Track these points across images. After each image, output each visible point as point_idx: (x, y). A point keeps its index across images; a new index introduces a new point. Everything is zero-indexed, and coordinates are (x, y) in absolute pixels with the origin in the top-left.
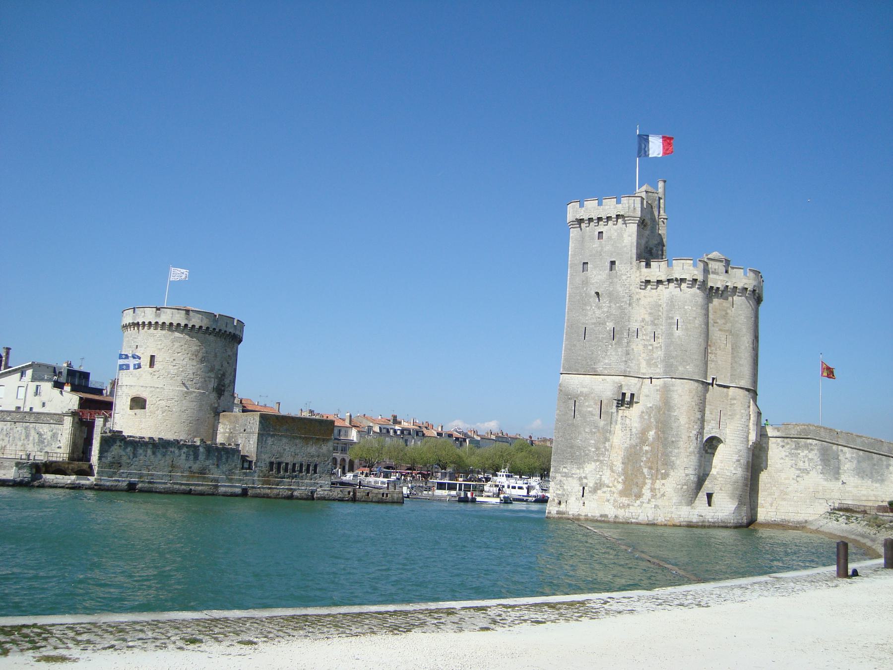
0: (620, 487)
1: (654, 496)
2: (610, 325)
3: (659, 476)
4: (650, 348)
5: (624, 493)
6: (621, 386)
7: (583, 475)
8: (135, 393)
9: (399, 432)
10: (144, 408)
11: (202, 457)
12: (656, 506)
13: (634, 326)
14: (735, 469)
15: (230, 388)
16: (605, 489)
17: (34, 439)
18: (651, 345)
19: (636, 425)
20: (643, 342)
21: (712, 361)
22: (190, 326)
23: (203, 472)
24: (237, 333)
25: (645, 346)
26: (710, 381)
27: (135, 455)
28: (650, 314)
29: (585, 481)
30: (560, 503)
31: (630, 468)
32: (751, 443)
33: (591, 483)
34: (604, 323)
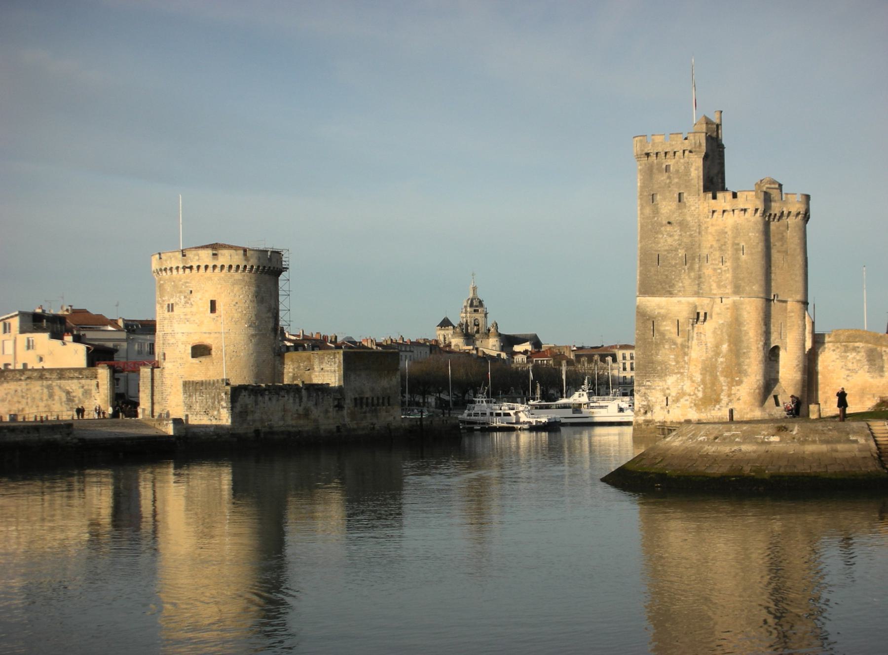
0: (700, 395)
1: (730, 401)
2: (681, 253)
4: (719, 271)
6: (696, 307)
7: (666, 387)
8: (197, 340)
11: (305, 399)
13: (705, 252)
17: (60, 399)
23: (306, 414)
25: (715, 270)
27: (256, 403)
29: (668, 392)
30: (646, 413)
32: (807, 350)
33: (673, 393)
34: (676, 250)
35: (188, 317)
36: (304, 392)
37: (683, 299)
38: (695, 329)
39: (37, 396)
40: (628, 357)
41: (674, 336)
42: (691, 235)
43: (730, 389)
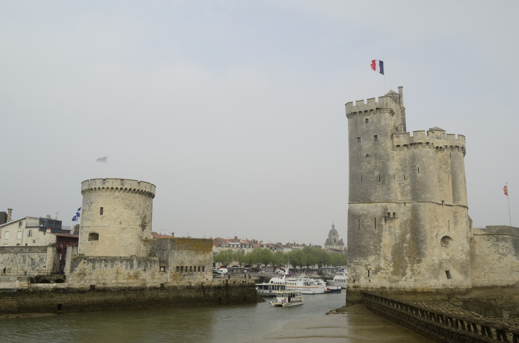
0: (391, 269)
2: (377, 173)
3: (416, 262)
4: (403, 185)
5: (395, 273)
7: (368, 263)
9: (239, 246)
12: (416, 280)
13: (391, 172)
14: (461, 255)
15: (149, 225)
16: (382, 271)
18: (403, 183)
19: (398, 231)
20: (398, 182)
21: (441, 191)
22: (124, 189)
23: (136, 276)
24: (152, 192)
25: (400, 184)
26: (441, 203)
27: (94, 268)
28: (401, 165)
29: (369, 267)
30: (354, 281)
31: (396, 257)
34: (373, 172)
36: (135, 262)
37: (379, 204)
38: (387, 224)
39: (18, 261)
41: (373, 228)
42: (382, 162)
43: (412, 266)
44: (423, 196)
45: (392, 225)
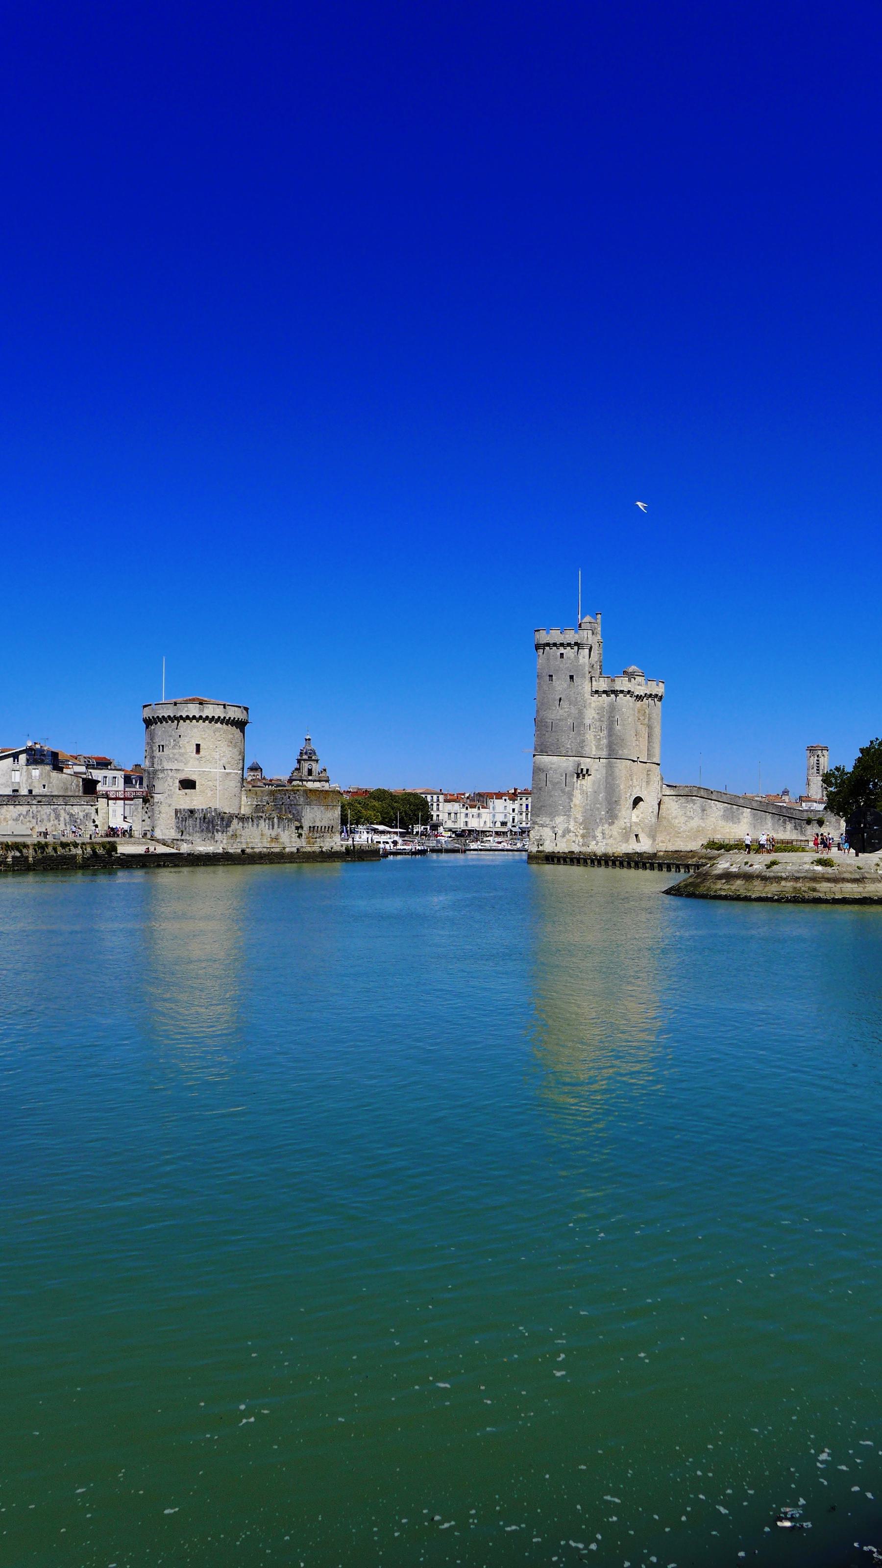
0: (581, 832)
2: (570, 721)
6: (579, 765)
8: (183, 776)
10: (195, 788)
11: (276, 826)
13: (587, 722)
17: (65, 820)
23: (276, 839)
25: (595, 736)
35: (176, 756)
39: (45, 817)
40: (435, 800)
44: (620, 752)
45: (584, 782)
